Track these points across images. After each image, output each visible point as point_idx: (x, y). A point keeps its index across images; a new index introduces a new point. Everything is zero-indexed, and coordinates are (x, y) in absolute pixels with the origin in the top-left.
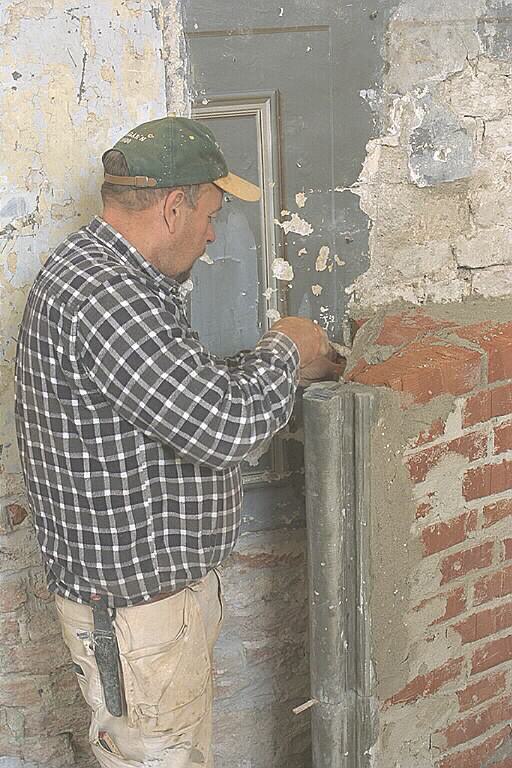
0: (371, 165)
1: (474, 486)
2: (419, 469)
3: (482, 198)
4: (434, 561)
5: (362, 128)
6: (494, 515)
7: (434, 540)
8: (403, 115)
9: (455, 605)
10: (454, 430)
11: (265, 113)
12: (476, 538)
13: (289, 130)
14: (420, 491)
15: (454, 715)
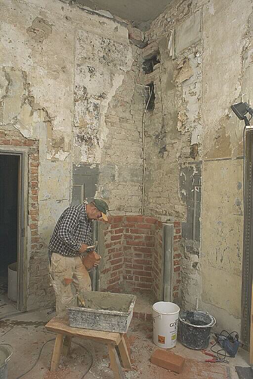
0: (96, 194)
1: (113, 238)
2: (106, 234)
3: (111, 200)
4: (107, 249)
5: (95, 189)
6: (115, 244)
7: (108, 246)
8: (100, 188)
9: (110, 258)
10: (110, 229)
11: (83, 185)
12: (113, 247)
13: (86, 188)
14: (105, 237)
15: (110, 278)
